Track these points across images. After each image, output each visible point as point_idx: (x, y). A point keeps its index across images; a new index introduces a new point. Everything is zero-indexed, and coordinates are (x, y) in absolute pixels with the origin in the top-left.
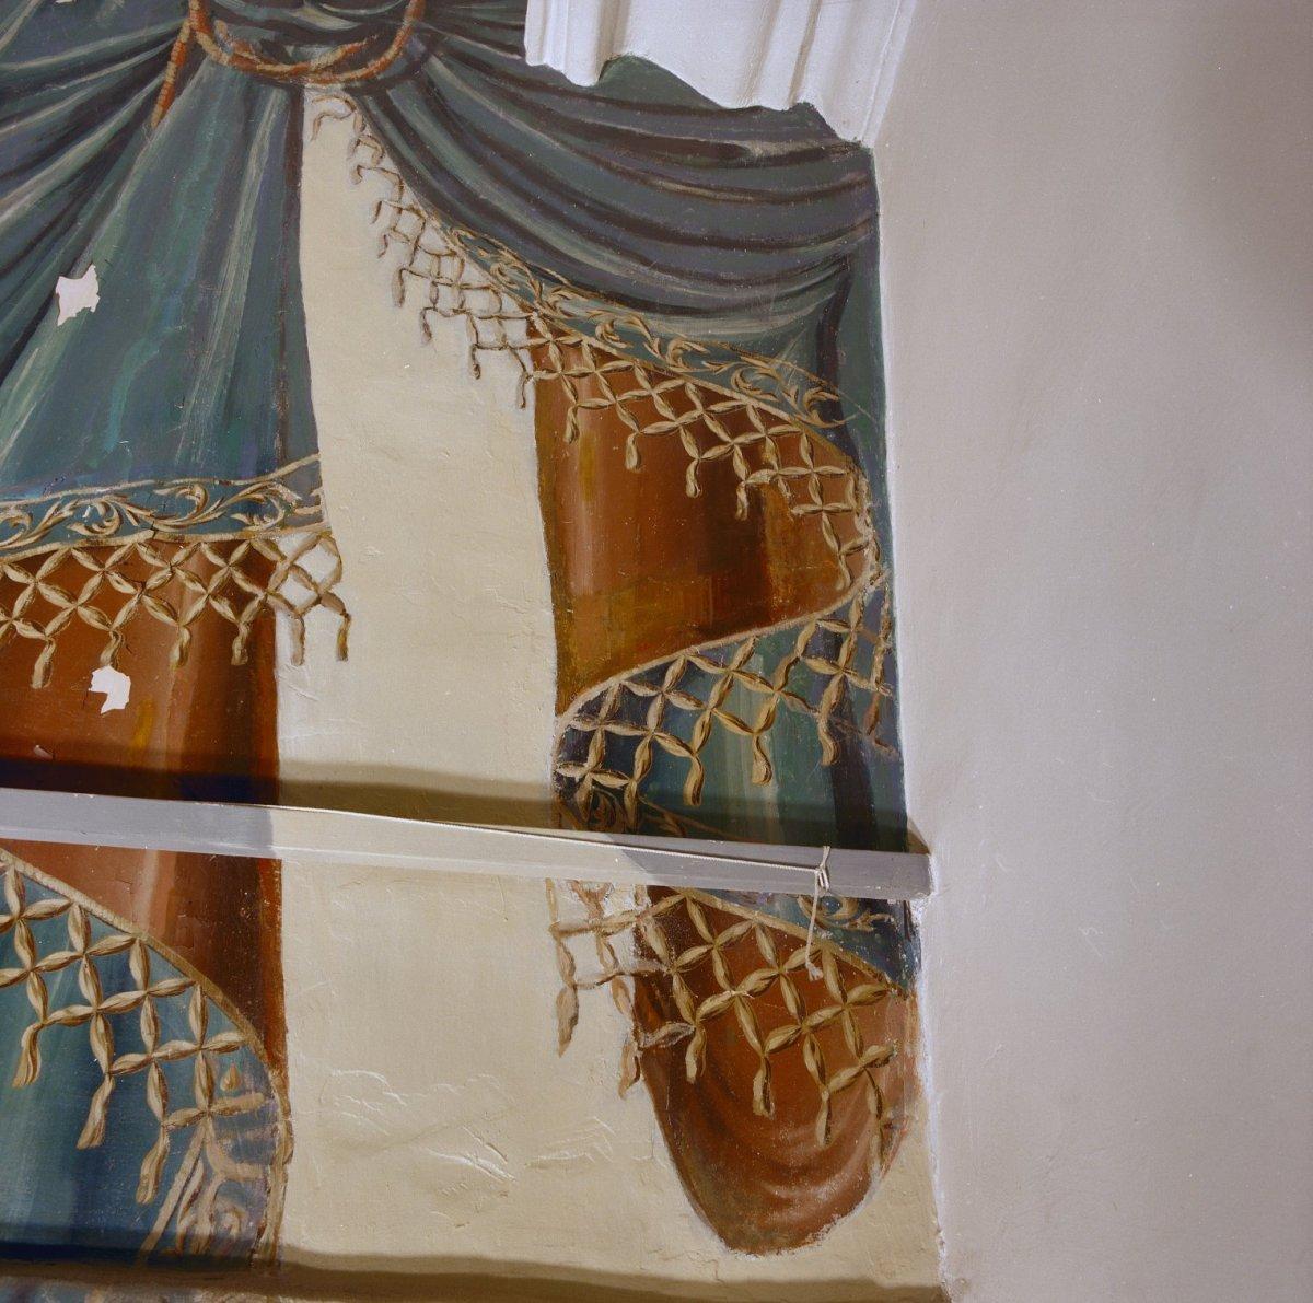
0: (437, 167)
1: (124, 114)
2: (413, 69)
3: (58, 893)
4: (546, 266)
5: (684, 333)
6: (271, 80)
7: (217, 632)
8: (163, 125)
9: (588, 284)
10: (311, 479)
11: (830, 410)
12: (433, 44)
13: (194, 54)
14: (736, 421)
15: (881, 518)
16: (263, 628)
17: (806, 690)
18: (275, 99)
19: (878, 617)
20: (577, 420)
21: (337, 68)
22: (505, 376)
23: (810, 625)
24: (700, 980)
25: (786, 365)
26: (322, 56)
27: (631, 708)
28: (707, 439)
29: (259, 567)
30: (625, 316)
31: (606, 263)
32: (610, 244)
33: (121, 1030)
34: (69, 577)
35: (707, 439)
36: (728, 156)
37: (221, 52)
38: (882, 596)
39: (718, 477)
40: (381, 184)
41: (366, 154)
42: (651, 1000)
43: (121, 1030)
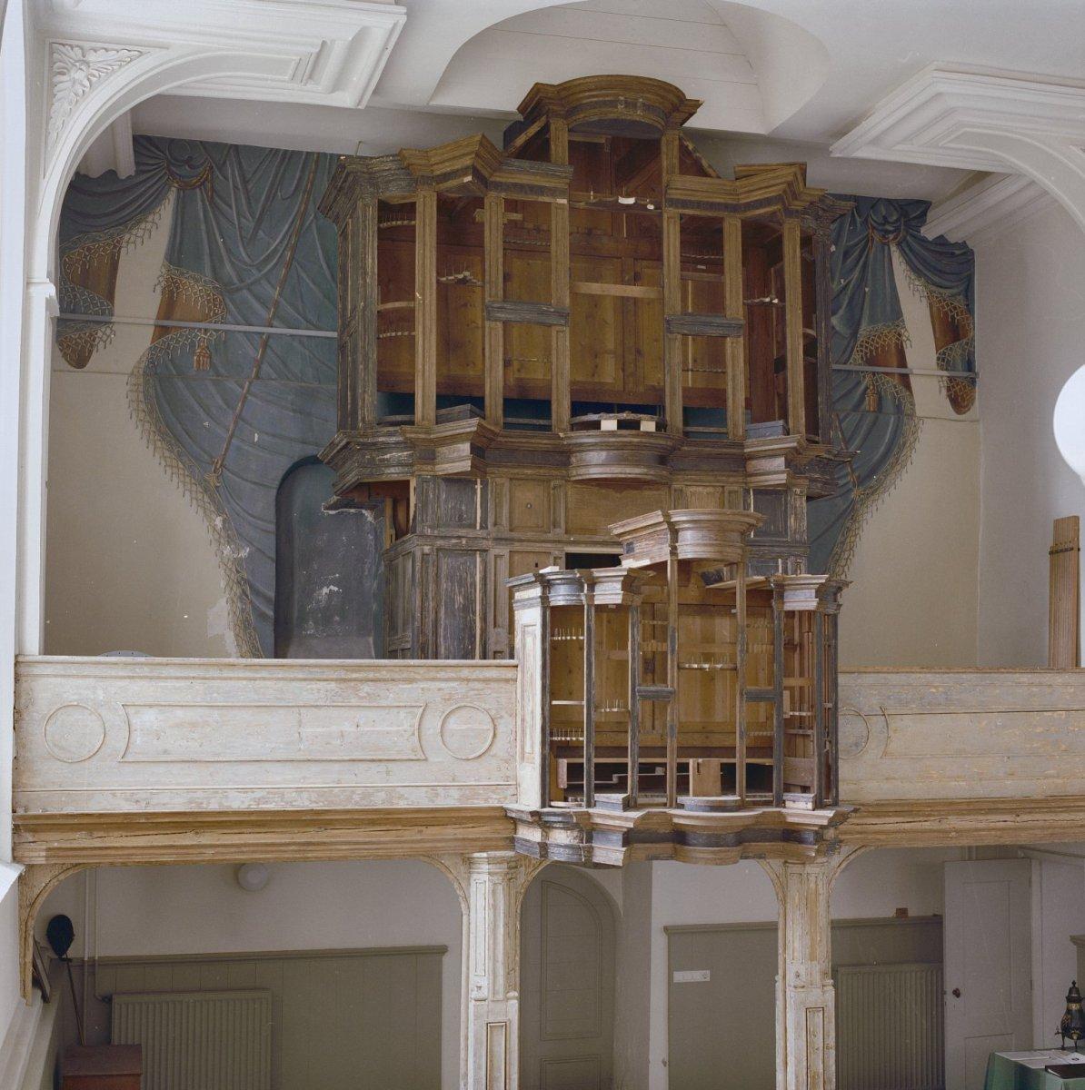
0: (910, 260)
1: (866, 253)
2: (905, 239)
3: (888, 378)
4: (929, 281)
5: (948, 292)
6: (885, 244)
7: (897, 344)
8: (871, 256)
9: (934, 284)
10: (903, 321)
11: (967, 305)
12: (907, 232)
13: (873, 240)
14: (955, 308)
15: (974, 323)
16: (902, 343)
17: (964, 351)
18: (886, 248)
19: (973, 340)
20: (934, 309)
21: (894, 239)
22: (924, 301)
23: (965, 341)
24: (953, 387)
25: (961, 297)
26: (891, 236)
27: (944, 353)
28: (951, 311)
29: (900, 335)
30: (941, 290)
31: (936, 279)
32: (936, 275)
33: (897, 392)
34: (879, 337)
35: (951, 311)
36: (953, 254)
37: (877, 237)
38: (974, 336)
39: (953, 317)
40: (904, 266)
41: (901, 259)
42: (949, 389)
43: (897, 392)
